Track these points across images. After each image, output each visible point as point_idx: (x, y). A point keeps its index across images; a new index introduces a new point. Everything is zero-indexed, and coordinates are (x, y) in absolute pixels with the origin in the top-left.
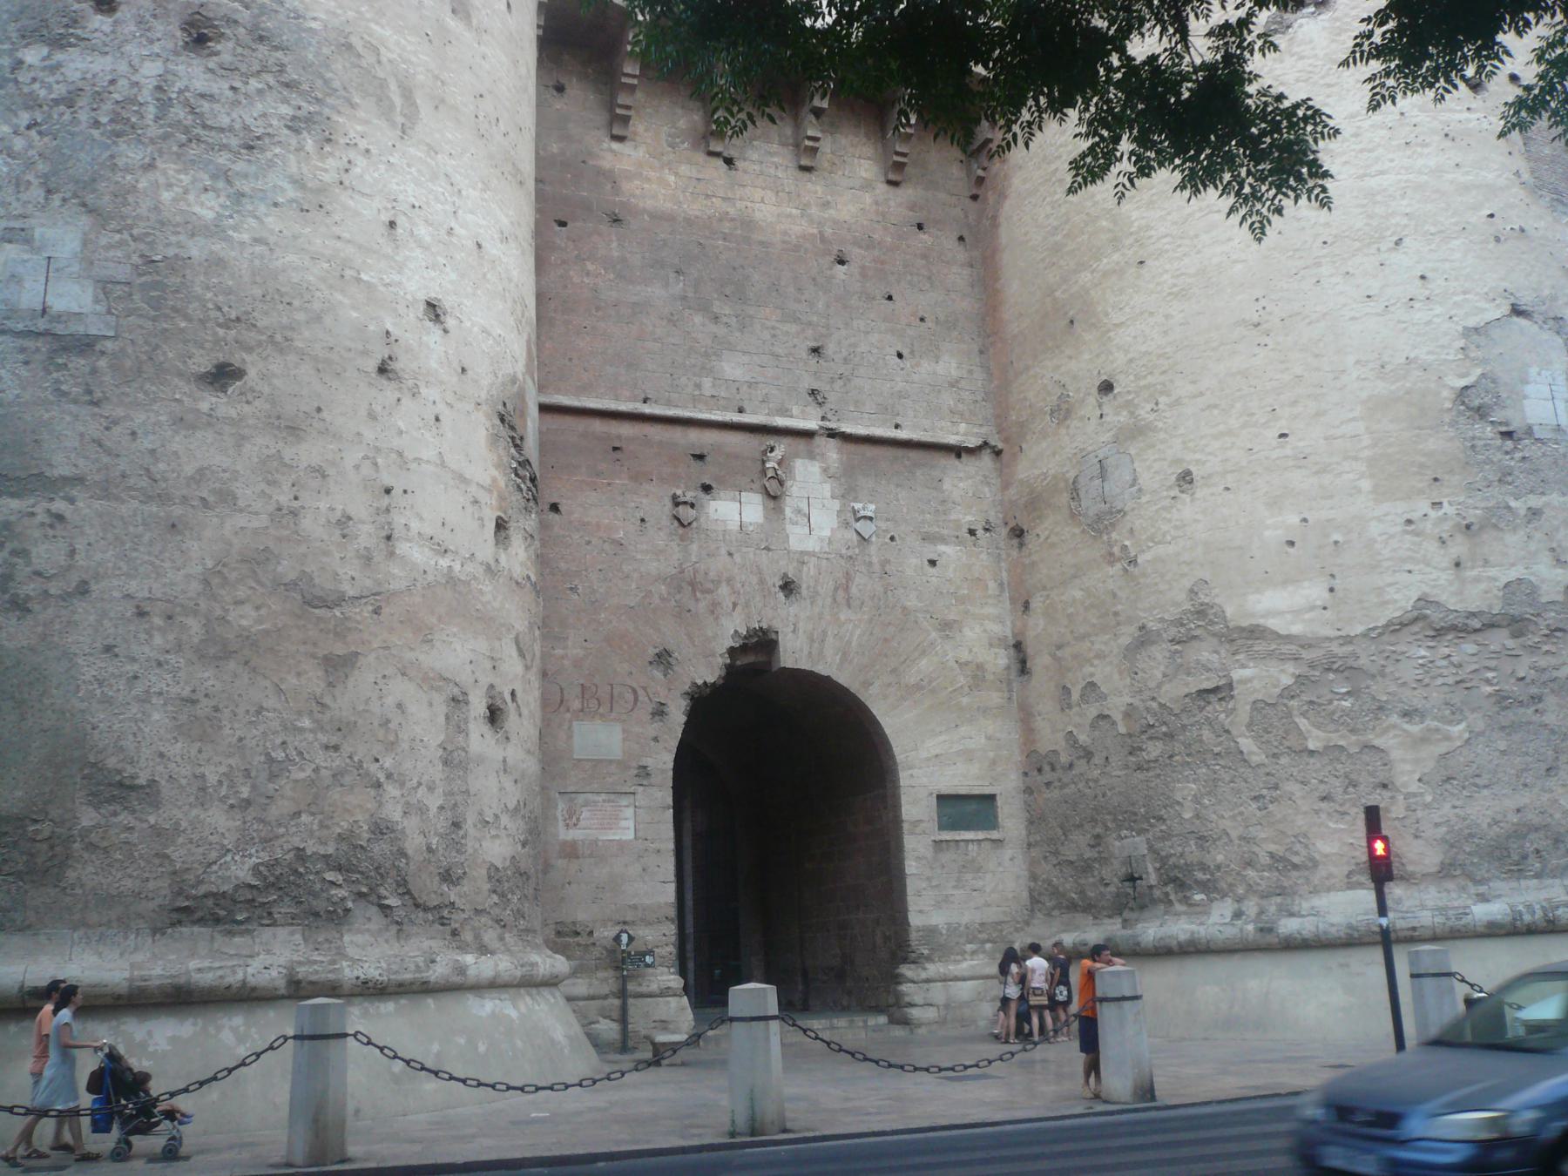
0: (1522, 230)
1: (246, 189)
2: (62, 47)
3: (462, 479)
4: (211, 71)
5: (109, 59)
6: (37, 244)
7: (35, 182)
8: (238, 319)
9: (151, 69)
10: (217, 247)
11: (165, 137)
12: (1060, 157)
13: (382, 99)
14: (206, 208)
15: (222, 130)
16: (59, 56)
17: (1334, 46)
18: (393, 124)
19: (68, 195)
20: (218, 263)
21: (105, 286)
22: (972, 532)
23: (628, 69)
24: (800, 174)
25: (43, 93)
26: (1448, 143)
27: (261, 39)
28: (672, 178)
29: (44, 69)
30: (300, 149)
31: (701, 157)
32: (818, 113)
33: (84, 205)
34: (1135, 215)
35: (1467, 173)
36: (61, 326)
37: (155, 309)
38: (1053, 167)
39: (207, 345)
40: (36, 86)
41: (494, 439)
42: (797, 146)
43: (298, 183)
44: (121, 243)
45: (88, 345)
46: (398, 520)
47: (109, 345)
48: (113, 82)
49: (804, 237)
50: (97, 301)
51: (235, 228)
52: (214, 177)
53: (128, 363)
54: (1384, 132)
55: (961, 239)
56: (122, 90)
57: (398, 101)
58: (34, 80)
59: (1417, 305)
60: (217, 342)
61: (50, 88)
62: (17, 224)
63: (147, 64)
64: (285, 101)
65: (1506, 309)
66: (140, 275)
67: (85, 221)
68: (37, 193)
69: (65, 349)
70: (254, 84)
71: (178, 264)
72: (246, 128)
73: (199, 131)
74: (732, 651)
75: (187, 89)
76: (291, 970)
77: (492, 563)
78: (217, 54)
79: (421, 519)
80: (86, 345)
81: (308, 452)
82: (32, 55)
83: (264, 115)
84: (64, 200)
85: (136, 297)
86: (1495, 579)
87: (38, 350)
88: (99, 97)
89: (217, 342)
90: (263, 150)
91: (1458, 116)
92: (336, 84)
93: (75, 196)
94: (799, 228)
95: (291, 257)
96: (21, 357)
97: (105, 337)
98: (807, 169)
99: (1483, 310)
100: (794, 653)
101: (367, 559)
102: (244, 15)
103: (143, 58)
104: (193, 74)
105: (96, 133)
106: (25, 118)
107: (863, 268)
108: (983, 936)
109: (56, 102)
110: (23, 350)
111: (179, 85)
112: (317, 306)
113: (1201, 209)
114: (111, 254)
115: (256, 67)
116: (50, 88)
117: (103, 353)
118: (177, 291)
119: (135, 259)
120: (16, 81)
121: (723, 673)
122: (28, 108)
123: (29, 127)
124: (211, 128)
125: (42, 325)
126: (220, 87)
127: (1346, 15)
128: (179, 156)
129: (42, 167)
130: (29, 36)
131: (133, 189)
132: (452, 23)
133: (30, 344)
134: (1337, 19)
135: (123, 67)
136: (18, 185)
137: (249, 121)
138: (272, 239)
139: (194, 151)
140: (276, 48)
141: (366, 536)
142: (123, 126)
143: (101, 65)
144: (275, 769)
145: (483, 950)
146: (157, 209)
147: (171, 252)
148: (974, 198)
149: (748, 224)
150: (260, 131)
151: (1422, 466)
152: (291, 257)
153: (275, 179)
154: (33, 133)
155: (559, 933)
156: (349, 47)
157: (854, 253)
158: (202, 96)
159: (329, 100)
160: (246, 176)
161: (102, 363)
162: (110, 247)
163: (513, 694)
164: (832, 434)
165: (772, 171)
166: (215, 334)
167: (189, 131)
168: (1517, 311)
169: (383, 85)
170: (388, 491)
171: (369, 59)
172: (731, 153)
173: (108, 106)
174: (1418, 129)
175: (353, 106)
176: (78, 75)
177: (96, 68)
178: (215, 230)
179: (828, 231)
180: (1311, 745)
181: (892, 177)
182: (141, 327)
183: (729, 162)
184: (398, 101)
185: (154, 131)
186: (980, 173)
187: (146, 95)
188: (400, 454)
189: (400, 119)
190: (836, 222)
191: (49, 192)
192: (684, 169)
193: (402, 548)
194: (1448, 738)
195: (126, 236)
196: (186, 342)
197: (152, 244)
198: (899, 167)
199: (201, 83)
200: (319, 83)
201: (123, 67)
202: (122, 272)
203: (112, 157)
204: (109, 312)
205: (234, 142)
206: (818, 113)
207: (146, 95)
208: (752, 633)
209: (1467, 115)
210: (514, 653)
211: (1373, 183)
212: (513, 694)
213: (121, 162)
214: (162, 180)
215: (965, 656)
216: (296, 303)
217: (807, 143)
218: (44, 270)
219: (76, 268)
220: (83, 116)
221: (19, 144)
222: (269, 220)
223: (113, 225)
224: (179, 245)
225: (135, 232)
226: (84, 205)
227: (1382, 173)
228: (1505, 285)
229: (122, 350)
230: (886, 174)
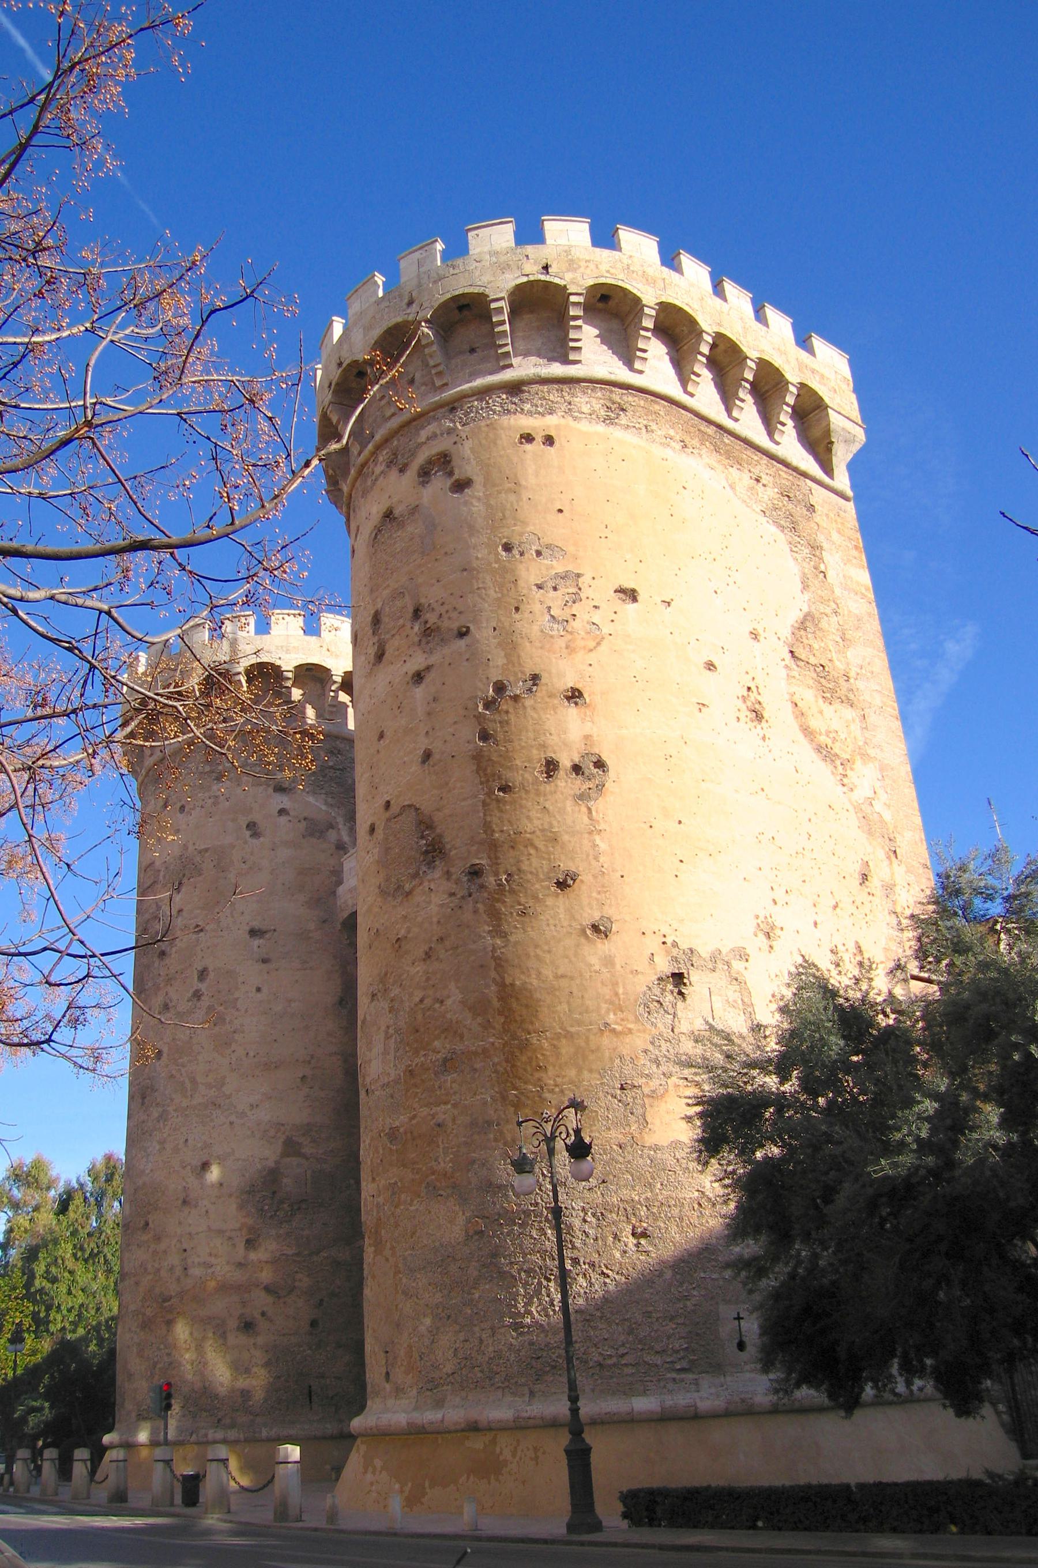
3: (221, 1232)
41: (241, 1207)
46: (189, 1261)
57: (188, 1085)
77: (243, 1261)
79: (199, 1256)
81: (163, 1246)
101: (178, 1280)
141: (178, 1271)
144: (155, 1364)
145: (232, 1426)
163: (263, 1314)
169: (183, 1083)
170: (185, 1250)
184: (188, 1085)
188: (190, 1234)
189: (189, 1093)
193: (191, 1271)
210: (263, 1294)
212: (263, 1314)
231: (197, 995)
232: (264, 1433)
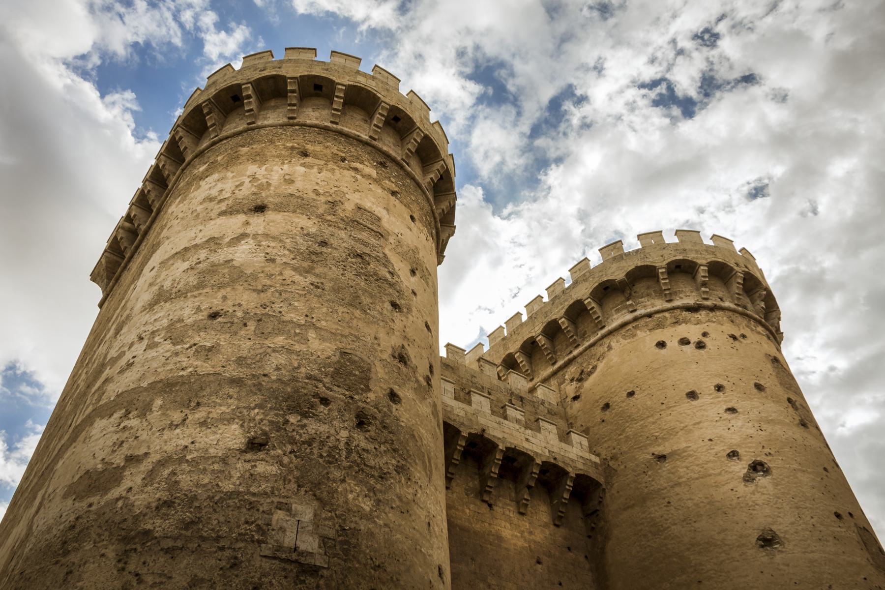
1: (381, 498)
2: (306, 417)
4: (367, 438)
5: (327, 426)
6: (293, 513)
7: (293, 480)
8: (379, 566)
9: (344, 434)
10: (371, 526)
11: (350, 467)
12: (642, 524)
13: (424, 462)
14: (367, 506)
15: (371, 467)
16: (305, 421)
19: (308, 489)
20: (371, 534)
21: (324, 540)
23: (455, 457)
24: (518, 516)
25: (298, 437)
26: (836, 542)
27: (384, 427)
28: (468, 511)
29: (298, 426)
30: (400, 482)
31: (478, 502)
32: (529, 487)
33: (315, 495)
34: (692, 557)
36: (303, 559)
37: (346, 555)
38: (639, 528)
39: (367, 578)
40: (295, 433)
42: (518, 502)
43: (400, 498)
44: (331, 518)
45: (315, 571)
47: (325, 572)
48: (328, 437)
49: (523, 548)
50: (320, 547)
51: (378, 517)
52: (369, 490)
53: (333, 584)
55: (586, 557)
56: (331, 442)
58: (294, 430)
60: (371, 577)
61: (301, 436)
62: (284, 501)
63: (342, 431)
64: (394, 458)
66: (339, 536)
67: (316, 504)
68: (293, 486)
69: (304, 572)
70: (383, 448)
71: (356, 531)
72: (380, 468)
73: (362, 466)
75: (358, 446)
78: (369, 431)
80: (314, 571)
82: (293, 419)
83: (387, 463)
84: (306, 491)
85: (338, 547)
87: (292, 570)
88: (322, 443)
89: (371, 577)
90: (387, 480)
92: (411, 453)
93: (311, 490)
94: (521, 543)
95: (399, 536)
96: (283, 573)
97: (324, 568)
98: (522, 514)
102: (379, 416)
103: (341, 428)
104: (360, 439)
105: (321, 460)
106: (289, 448)
107: (548, 566)
109: (304, 443)
110: (284, 569)
111: (355, 443)
112: (408, 563)
113: (728, 559)
114: (327, 523)
115: (383, 440)
116: (301, 436)
117: (322, 576)
118: (355, 547)
119: (337, 526)
120: (285, 429)
122: (291, 443)
123: (290, 453)
124: (367, 466)
125: (294, 556)
126: (370, 447)
128: (356, 477)
129: (296, 473)
130: (293, 409)
131: (336, 491)
133: (288, 567)
135: (332, 431)
136: (284, 481)
137: (382, 465)
138: (391, 525)
139: (361, 476)
140: (390, 432)
142: (332, 460)
143: (324, 428)
146: (346, 502)
147: (353, 525)
148: (589, 537)
149: (500, 538)
150: (386, 470)
152: (399, 536)
153: (390, 496)
154: (292, 456)
156: (414, 436)
157: (544, 559)
158: (364, 450)
159: (409, 460)
160: (381, 492)
161: (322, 582)
162: (326, 519)
165: (508, 513)
166: (370, 573)
167: (359, 468)
171: (419, 443)
172: (492, 502)
173: (326, 448)
175: (416, 464)
176: (314, 431)
177: (321, 429)
178: (369, 517)
179: (533, 546)
181: (557, 523)
182: (339, 564)
183: (490, 506)
185: (345, 464)
186: (593, 525)
187: (342, 446)
190: (535, 542)
191: (299, 486)
192: (472, 506)
195: (333, 514)
196: (358, 575)
197: (344, 520)
198: (560, 518)
199: (363, 444)
200: (405, 452)
201: (332, 431)
202: (331, 533)
203: (328, 473)
204: (325, 554)
205: (376, 474)
206: (529, 487)
207: (342, 446)
209: (839, 529)
211: (811, 556)
213: (331, 476)
214: (348, 488)
216: (401, 560)
217: (525, 502)
218: (296, 527)
219: (311, 528)
220: (315, 451)
221: (286, 460)
222: (390, 515)
223: (328, 508)
224: (356, 523)
225: (337, 512)
226: (315, 495)
227: (812, 552)
229: (331, 576)
230: (553, 521)
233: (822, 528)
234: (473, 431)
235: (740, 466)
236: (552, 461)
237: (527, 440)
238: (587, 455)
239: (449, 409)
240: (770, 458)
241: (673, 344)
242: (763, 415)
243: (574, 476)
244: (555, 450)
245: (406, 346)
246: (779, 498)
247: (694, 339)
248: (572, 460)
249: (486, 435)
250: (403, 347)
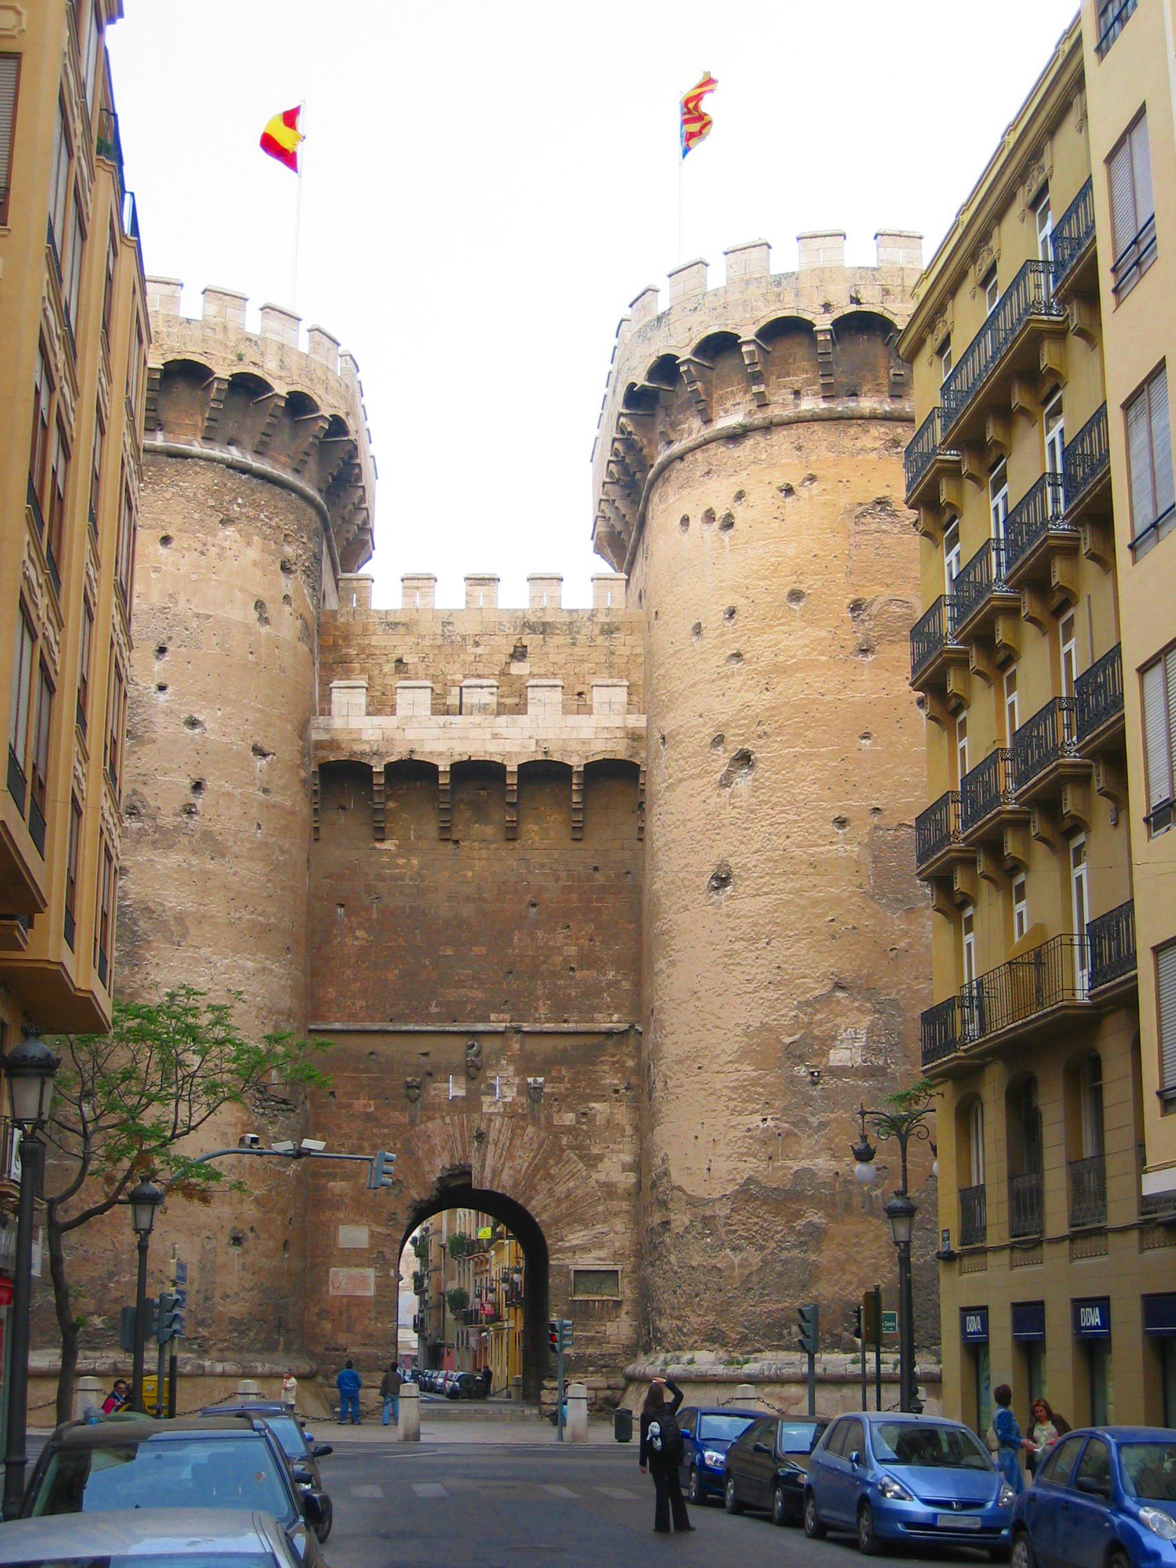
0: (854, 928)
17: (753, 800)
18: (173, 943)
22: (616, 1091)
26: (812, 870)
32: (511, 804)
35: (820, 891)
54: (771, 864)
59: (772, 987)
65: (828, 988)
74: (440, 1179)
76: (115, 1364)
86: (791, 1168)
91: (822, 849)
99: (813, 989)
100: (483, 1179)
108: (602, 1362)
121: (435, 1193)
127: (762, 777)
132: (211, 866)
134: (756, 780)
148: (641, 840)
151: (760, 1094)
155: (327, 1349)
156: (148, 908)
164: (518, 1031)
168: (839, 986)
174: (793, 861)
180: (694, 1264)
183: (456, 842)
186: (640, 824)
194: (751, 1265)
208: (454, 1167)
215: (602, 1177)
227: (766, 893)
228: (832, 969)
231: (189, 810)
232: (260, 1370)
233: (798, 852)
234: (393, 759)
235: (722, 762)
236: (540, 757)
237: (495, 736)
238: (617, 721)
239: (354, 736)
240: (761, 742)
241: (696, 523)
242: (781, 659)
243: (581, 769)
244: (551, 735)
245: (140, 788)
246: (752, 811)
247: (720, 514)
248: (584, 742)
249: (416, 757)
250: (135, 792)
